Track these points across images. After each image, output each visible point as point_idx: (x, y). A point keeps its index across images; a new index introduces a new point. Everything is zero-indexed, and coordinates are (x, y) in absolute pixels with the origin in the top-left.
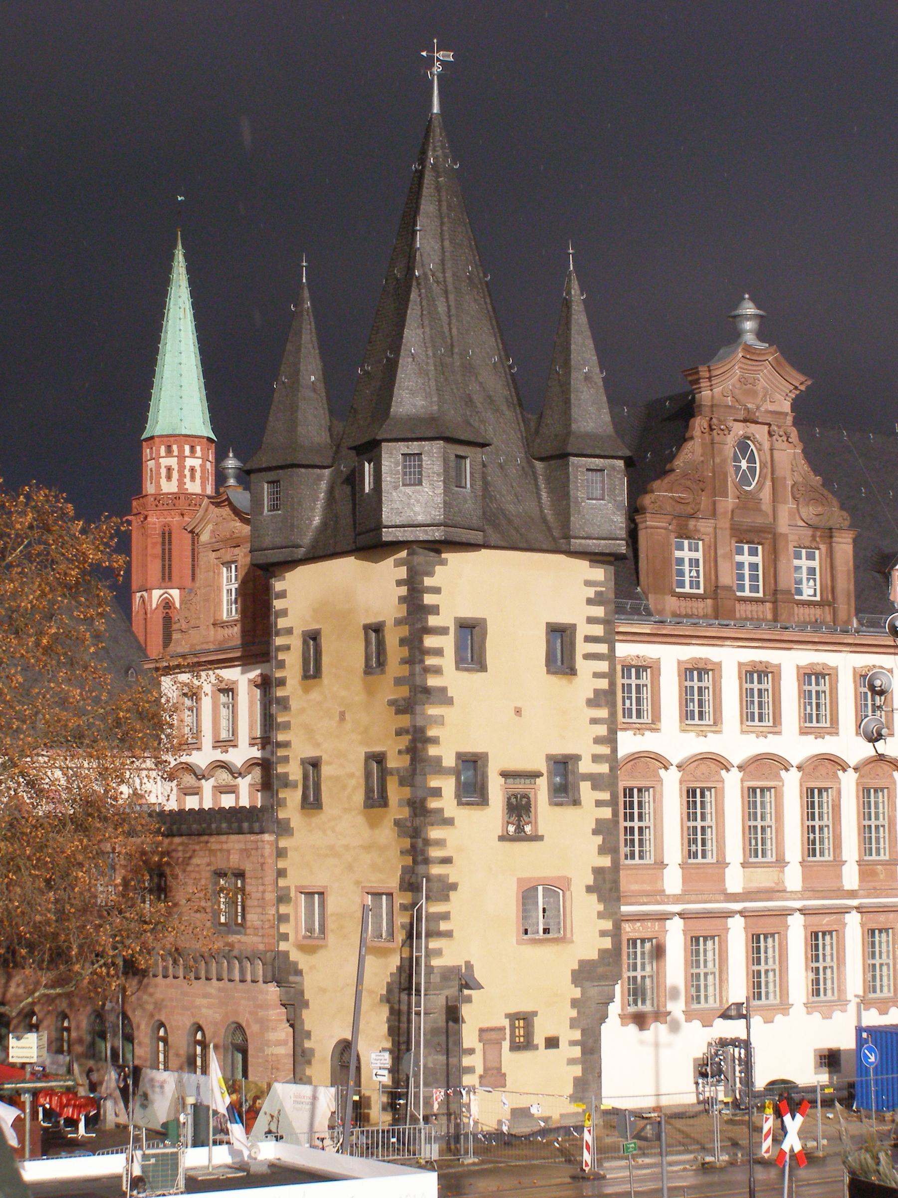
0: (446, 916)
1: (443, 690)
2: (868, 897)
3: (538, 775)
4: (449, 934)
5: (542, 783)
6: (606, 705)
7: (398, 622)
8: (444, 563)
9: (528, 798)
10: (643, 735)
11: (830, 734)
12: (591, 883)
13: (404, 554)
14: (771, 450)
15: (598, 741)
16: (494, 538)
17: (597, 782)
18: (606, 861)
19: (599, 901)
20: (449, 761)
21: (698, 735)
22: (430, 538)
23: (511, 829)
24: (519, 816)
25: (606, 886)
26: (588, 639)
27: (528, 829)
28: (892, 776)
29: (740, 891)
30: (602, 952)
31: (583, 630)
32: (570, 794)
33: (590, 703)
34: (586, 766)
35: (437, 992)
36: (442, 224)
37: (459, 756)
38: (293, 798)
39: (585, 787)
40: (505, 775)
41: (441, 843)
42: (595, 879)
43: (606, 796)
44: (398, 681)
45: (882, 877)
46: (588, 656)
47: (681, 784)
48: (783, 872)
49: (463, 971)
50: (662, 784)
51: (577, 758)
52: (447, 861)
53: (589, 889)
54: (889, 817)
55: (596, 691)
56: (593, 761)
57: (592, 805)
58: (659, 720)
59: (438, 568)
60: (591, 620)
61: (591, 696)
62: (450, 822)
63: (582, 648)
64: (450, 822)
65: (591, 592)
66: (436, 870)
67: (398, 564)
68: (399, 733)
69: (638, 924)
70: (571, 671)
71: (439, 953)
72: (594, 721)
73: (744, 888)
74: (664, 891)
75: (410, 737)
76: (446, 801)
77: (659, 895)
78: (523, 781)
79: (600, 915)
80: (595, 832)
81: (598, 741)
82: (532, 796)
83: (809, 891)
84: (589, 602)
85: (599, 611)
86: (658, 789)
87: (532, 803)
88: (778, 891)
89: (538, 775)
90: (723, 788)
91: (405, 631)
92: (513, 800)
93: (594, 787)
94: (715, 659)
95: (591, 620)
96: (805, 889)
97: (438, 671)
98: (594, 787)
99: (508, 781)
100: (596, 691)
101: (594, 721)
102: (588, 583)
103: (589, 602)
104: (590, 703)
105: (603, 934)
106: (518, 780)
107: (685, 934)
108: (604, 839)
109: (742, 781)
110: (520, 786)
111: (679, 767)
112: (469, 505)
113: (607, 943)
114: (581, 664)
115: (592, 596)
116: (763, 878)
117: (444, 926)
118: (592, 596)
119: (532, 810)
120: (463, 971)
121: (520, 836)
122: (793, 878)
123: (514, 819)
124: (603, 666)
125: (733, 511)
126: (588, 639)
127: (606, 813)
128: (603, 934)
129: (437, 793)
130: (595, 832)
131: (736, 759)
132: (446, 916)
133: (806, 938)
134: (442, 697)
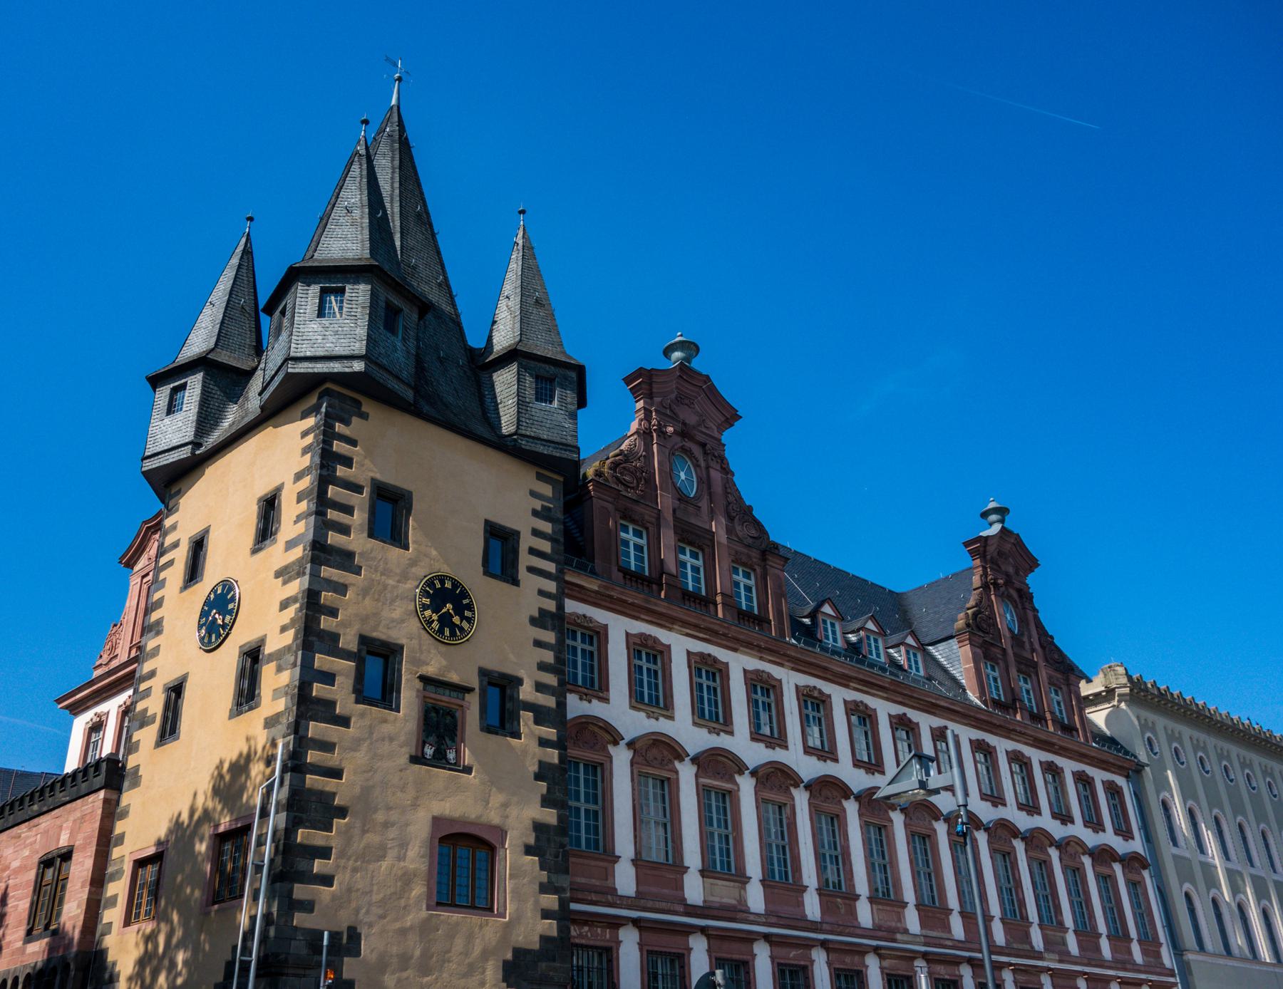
0: (325, 853)
1: (350, 555)
2: (831, 933)
3: (469, 690)
4: (327, 880)
5: (473, 701)
6: (553, 630)
7: (299, 477)
8: (364, 416)
9: (453, 716)
10: (590, 702)
11: (780, 746)
12: (532, 841)
13: (313, 400)
14: (708, 467)
15: (542, 667)
16: (426, 409)
17: (541, 716)
18: (550, 816)
19: (542, 868)
20: (349, 641)
21: (649, 717)
22: (347, 370)
23: (429, 751)
24: (440, 739)
25: (550, 846)
26: (533, 551)
27: (451, 756)
28: (840, 802)
29: (701, 904)
30: (544, 939)
31: (527, 541)
32: (507, 726)
33: (534, 621)
34: (526, 692)
35: (302, 972)
36: (393, 173)
37: (364, 640)
38: (147, 736)
39: (526, 717)
40: (424, 679)
41: (328, 747)
42: (537, 839)
43: (550, 733)
44: (290, 545)
45: (843, 911)
46: (531, 570)
47: (632, 765)
48: (745, 889)
49: (345, 941)
50: (611, 762)
51: (519, 681)
52: (336, 773)
53: (529, 850)
54: (842, 847)
55: (541, 611)
56: (537, 691)
57: (530, 744)
58: (608, 690)
59: (355, 420)
60: (536, 533)
61: (536, 614)
62: (344, 721)
63: (525, 560)
64: (344, 721)
65: (538, 505)
66: (311, 780)
67: (304, 416)
68: (284, 605)
69: (586, 929)
70: (515, 582)
71: (308, 906)
72: (538, 644)
73: (705, 901)
74: (616, 890)
75: (298, 605)
76: (341, 694)
77: (609, 894)
78: (447, 692)
79: (544, 888)
80: (538, 777)
81: (542, 667)
82: (458, 715)
83: (771, 916)
84: (535, 513)
85: (547, 527)
86: (607, 766)
87: (459, 724)
88: (741, 911)
89: (469, 690)
90: (678, 779)
91: (306, 482)
92: (433, 715)
93: (537, 722)
94: (664, 641)
95: (536, 533)
96: (768, 913)
97: (345, 530)
98: (537, 722)
99: (429, 687)
100: (541, 611)
101: (538, 644)
102: (533, 494)
103: (535, 513)
104: (534, 621)
105: (546, 914)
106: (441, 690)
107: (641, 950)
108: (548, 789)
109: (697, 776)
110: (445, 698)
111: (630, 745)
112: (400, 355)
113: (550, 927)
114: (523, 573)
115: (539, 508)
116: (724, 893)
117: (318, 866)
118: (539, 508)
119: (459, 733)
120: (345, 941)
121: (439, 760)
122: (756, 898)
123: (432, 739)
124: (551, 586)
125: (674, 511)
126: (533, 551)
127: (553, 756)
128: (546, 914)
129: (329, 678)
130: (538, 777)
131: (692, 750)
132: (325, 853)
133: (774, 973)
134: (345, 559)
